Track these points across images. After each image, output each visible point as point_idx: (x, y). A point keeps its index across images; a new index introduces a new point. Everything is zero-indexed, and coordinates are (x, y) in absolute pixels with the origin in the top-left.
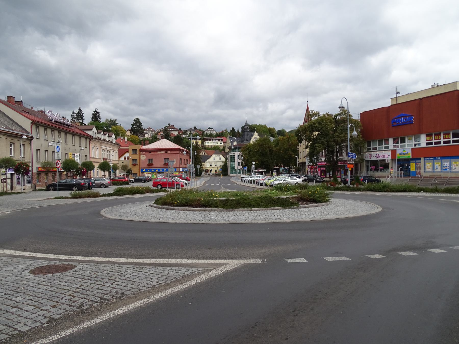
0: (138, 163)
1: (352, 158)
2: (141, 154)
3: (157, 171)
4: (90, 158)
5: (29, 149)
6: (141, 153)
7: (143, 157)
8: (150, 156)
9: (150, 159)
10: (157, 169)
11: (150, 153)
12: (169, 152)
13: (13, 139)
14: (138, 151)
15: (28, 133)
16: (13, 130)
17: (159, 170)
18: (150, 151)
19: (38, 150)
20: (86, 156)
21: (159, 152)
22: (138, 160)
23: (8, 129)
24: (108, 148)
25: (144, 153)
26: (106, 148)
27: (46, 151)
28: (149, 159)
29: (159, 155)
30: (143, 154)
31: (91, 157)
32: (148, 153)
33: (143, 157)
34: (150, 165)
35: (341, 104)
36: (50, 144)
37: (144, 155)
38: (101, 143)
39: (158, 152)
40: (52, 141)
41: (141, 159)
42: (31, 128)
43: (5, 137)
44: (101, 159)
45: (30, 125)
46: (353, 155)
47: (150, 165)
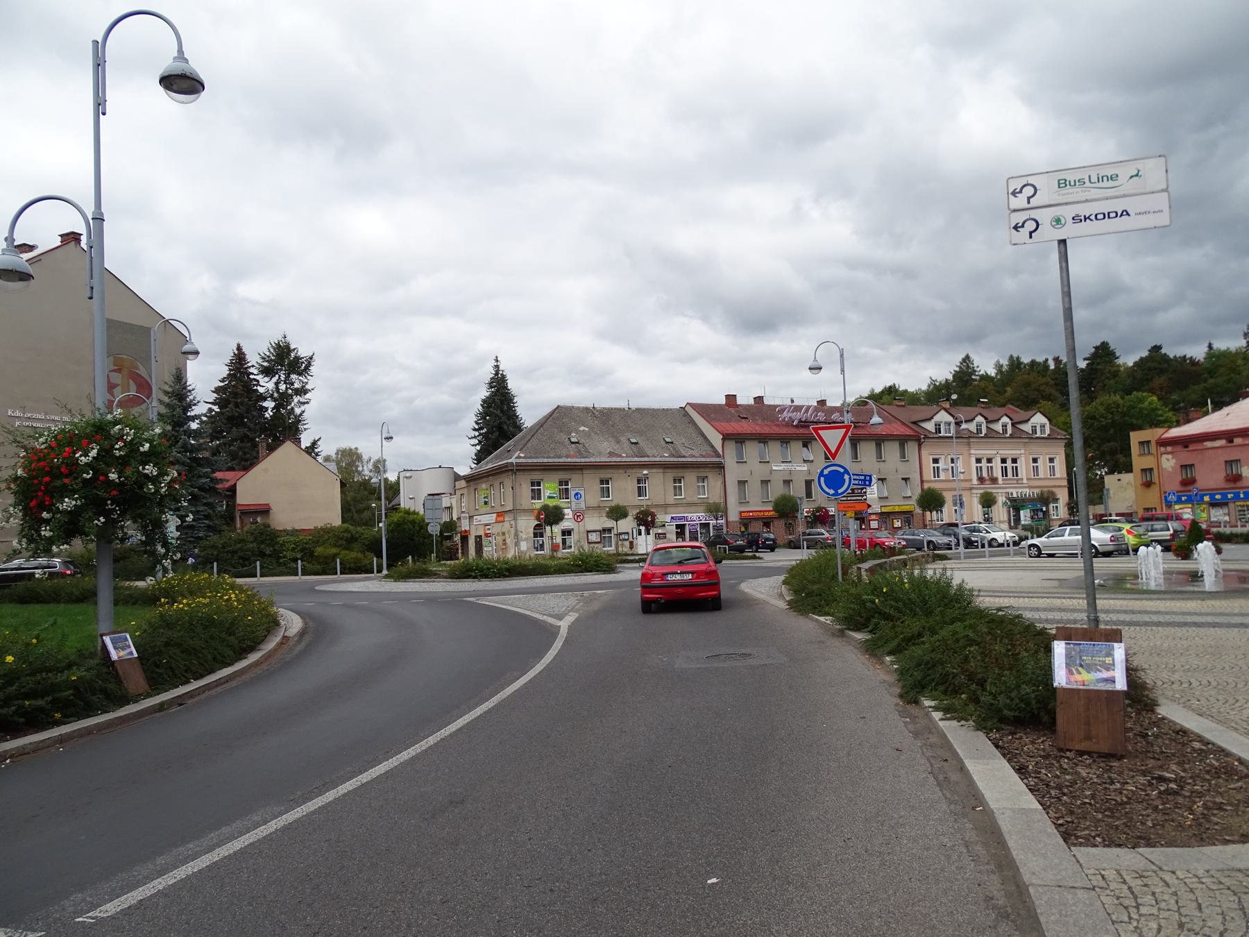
0: (1155, 479)
1: (859, 485)
2: (1162, 454)
3: (1207, 499)
4: (922, 482)
5: (719, 483)
6: (1163, 449)
7: (1168, 462)
8: (1186, 457)
9: (1186, 466)
10: (1206, 495)
11: (1186, 447)
12: (1238, 441)
13: (680, 470)
14: (1153, 444)
15: (718, 455)
16: (684, 457)
17: (1212, 496)
18: (1185, 442)
19: (742, 483)
20: (906, 479)
21: (1209, 444)
22: (1155, 471)
23: (674, 456)
24: (1001, 452)
25: (1169, 449)
26: (995, 452)
27: (765, 482)
28: (1184, 467)
29: (1210, 451)
30: (1168, 453)
31: (924, 479)
32: (1179, 448)
33: (1168, 460)
34: (1188, 482)
35: (815, 360)
36: (774, 468)
37: (1170, 456)
38: (969, 445)
39: (1205, 443)
40: (783, 462)
41: (1164, 466)
42: (723, 447)
43: (661, 470)
44: (971, 480)
45: (721, 442)
46: (863, 478)
47: (1188, 482)
